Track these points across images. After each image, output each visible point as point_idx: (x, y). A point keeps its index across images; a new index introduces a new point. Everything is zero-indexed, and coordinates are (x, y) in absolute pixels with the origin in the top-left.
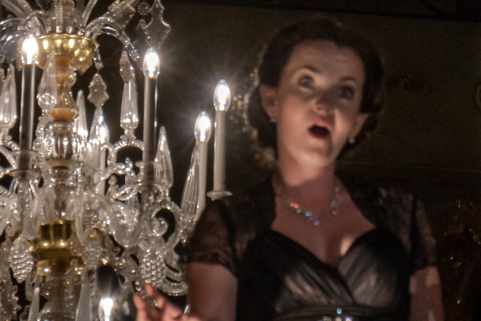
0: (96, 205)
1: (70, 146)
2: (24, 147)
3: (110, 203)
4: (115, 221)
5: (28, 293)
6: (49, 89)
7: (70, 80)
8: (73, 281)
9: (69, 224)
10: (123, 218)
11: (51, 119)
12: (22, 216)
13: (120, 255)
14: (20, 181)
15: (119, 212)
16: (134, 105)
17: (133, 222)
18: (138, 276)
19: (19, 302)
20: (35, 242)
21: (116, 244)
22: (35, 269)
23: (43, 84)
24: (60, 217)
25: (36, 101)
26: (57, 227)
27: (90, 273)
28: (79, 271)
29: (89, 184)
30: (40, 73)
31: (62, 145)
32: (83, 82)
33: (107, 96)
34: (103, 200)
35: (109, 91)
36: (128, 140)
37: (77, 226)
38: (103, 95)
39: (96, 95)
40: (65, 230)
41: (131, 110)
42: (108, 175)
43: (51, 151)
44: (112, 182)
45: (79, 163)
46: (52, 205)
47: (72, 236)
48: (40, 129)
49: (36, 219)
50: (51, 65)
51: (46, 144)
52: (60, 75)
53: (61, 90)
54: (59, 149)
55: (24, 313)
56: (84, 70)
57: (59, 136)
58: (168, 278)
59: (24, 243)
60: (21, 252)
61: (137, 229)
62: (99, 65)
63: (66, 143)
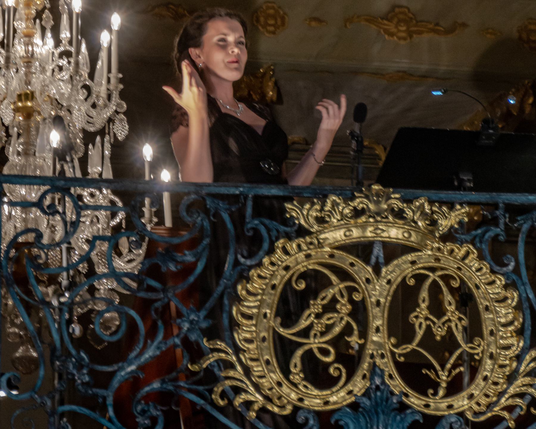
0: (47, 82)
1: (33, 50)
2: (8, 51)
3: (55, 81)
4: (58, 91)
5: (10, 131)
6: (21, 19)
7: (32, 14)
8: (35, 124)
9: (32, 93)
10: (62, 89)
11: (22, 35)
12: (7, 89)
13: (61, 109)
14: (6, 70)
15: (60, 86)
16: (68, 27)
17: (68, 91)
18: (71, 121)
19: (6, 137)
20: (15, 103)
21: (59, 103)
22: (14, 117)
23: (17, 16)
24: (28, 89)
25: (14, 25)
26: (26, 95)
27: (44, 119)
28: (39, 118)
29: (43, 70)
30: (15, 10)
31: (28, 49)
32: (39, 15)
33: (52, 22)
34: (51, 79)
35: (53, 20)
36: (65, 46)
37: (37, 94)
38: (50, 21)
39: (46, 22)
40: (30, 96)
41: (66, 30)
42: (53, 66)
43: (22, 53)
44: (56, 70)
45: (37, 59)
46: (23, 83)
47: (34, 99)
48: (16, 41)
49: (14, 91)
50: (21, 6)
51: (19, 49)
52: (27, 11)
53: (27, 19)
54: (27, 52)
55: (9, 142)
56: (40, 8)
57: (27, 44)
58: (88, 122)
59: (9, 104)
60: (7, 108)
61: (70, 95)
62: (48, 6)
63: (30, 49)
